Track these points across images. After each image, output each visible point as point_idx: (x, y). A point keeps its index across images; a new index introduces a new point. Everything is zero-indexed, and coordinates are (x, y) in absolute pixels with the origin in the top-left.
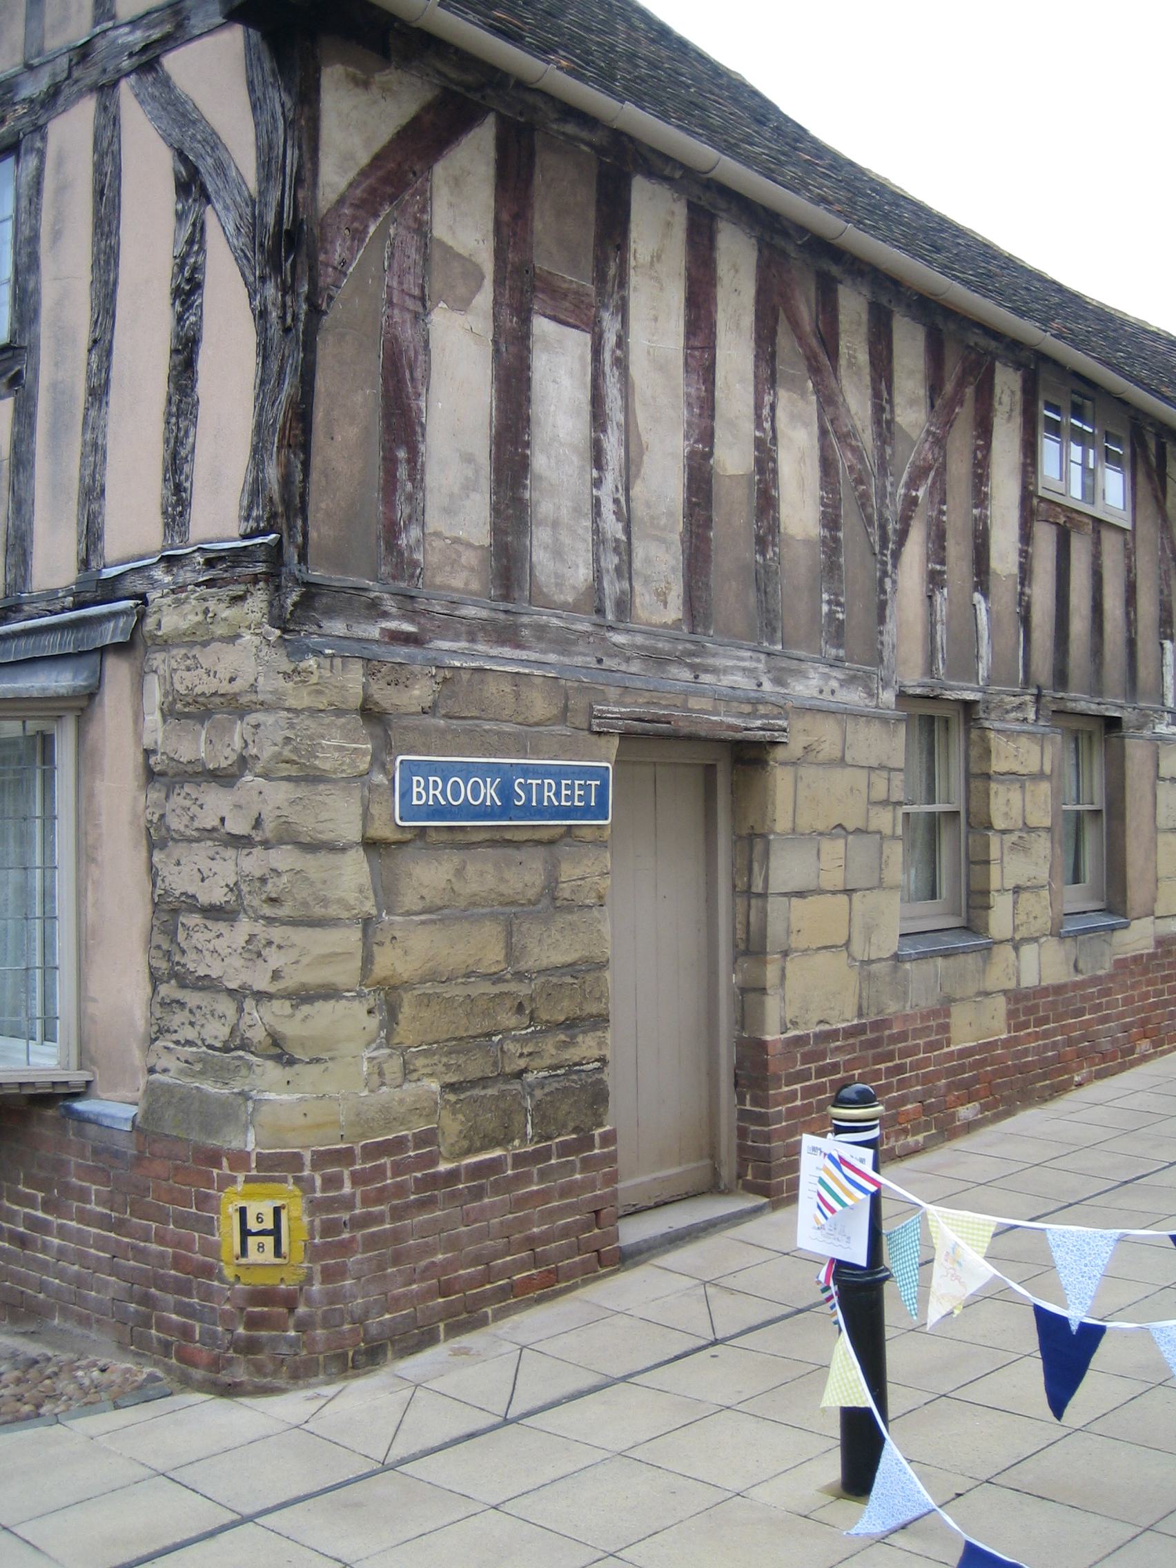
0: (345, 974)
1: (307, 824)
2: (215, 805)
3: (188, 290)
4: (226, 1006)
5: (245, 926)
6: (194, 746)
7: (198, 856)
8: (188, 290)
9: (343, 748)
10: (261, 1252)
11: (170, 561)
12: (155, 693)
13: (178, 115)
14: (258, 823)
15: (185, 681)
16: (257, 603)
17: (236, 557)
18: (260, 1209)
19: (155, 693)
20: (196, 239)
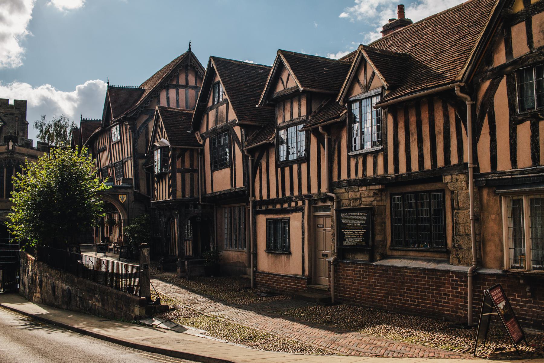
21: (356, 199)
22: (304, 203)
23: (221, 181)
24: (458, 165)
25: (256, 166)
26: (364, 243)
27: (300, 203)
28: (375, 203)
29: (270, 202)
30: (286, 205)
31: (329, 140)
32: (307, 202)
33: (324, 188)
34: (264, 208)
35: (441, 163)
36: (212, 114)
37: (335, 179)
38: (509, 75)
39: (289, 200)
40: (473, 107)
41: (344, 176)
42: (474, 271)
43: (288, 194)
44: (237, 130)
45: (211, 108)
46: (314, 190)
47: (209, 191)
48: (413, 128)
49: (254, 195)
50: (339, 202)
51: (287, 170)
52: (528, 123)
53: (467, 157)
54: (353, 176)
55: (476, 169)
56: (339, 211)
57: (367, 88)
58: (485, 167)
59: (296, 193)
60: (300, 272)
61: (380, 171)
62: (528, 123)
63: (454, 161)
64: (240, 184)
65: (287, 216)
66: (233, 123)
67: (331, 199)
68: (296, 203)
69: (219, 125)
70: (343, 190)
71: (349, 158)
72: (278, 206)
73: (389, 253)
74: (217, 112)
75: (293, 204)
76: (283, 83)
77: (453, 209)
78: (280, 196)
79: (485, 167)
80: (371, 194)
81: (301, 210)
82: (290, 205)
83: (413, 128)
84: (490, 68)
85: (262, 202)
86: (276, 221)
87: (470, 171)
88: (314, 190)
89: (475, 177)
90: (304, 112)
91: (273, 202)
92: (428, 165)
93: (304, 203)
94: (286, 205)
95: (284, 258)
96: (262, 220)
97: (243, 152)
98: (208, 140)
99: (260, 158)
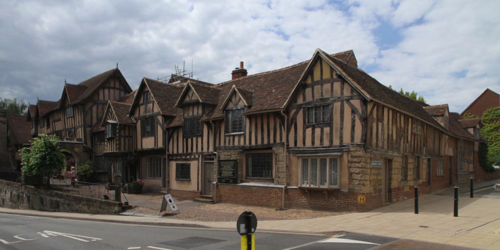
0: (368, 179)
1: (367, 167)
2: (357, 165)
3: (353, 121)
4: (358, 181)
5: (360, 175)
6: (356, 160)
7: (356, 169)
8: (353, 121)
9: (369, 161)
10: (362, 201)
11: (352, 145)
12: (350, 155)
13: (352, 106)
14: (362, 166)
15: (354, 154)
16: (362, 149)
17: (360, 145)
18: (362, 198)
19: (350, 155)
20: (354, 117)
21: (229, 155)
22: (199, 156)
23: (148, 143)
24: (280, 143)
25: (171, 137)
26: (232, 175)
27: (197, 156)
28: (238, 158)
29: (177, 155)
30: (188, 157)
31: (215, 127)
32: (201, 156)
33: (211, 149)
34: (174, 158)
35: (272, 141)
36: (142, 108)
37: (217, 145)
38: (304, 108)
39: (191, 154)
40: (288, 119)
41: (222, 144)
42: (286, 187)
43: (189, 151)
44: (160, 118)
45: (142, 105)
46: (205, 150)
47: (139, 147)
48: (259, 126)
49: (168, 151)
50: (219, 157)
51: (190, 141)
52: (310, 129)
53: (284, 140)
54: (227, 145)
55: (288, 145)
56: (219, 161)
57: (236, 105)
58: (292, 144)
59: (194, 151)
60: (196, 189)
61: (242, 143)
62: (310, 129)
63: (278, 141)
64: (160, 145)
65: (189, 162)
66: (158, 114)
67: (215, 155)
68: (195, 156)
69: (148, 114)
70: (221, 151)
71: (225, 136)
72: (183, 157)
73: (244, 180)
74: (146, 107)
75: (193, 157)
76: (189, 97)
77: (276, 161)
78: (185, 152)
79: (292, 144)
80: (236, 153)
81: (198, 159)
82: (191, 157)
83: (259, 126)
84: (296, 104)
85: (173, 155)
86: (182, 165)
87: (285, 146)
88: (205, 150)
89: (287, 148)
90: (200, 112)
91: (181, 155)
92: (266, 142)
93: (199, 156)
94: (188, 157)
95: (186, 182)
96: (173, 165)
97: (163, 129)
98: (139, 121)
99: (173, 133)
